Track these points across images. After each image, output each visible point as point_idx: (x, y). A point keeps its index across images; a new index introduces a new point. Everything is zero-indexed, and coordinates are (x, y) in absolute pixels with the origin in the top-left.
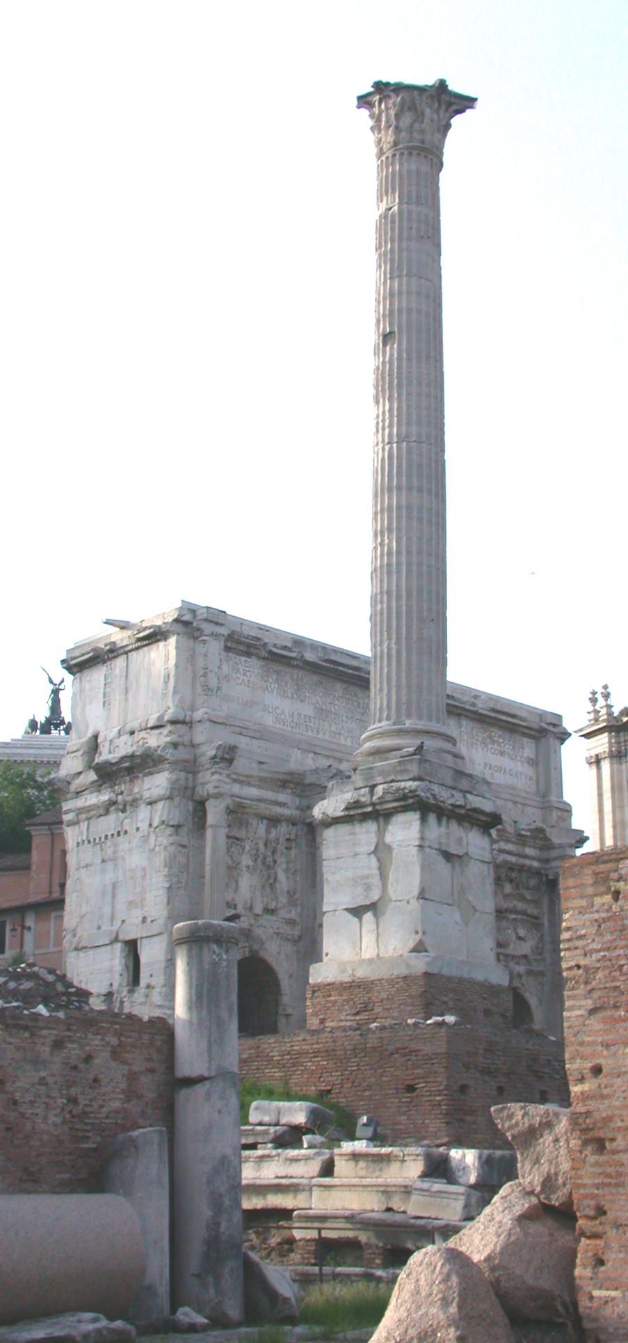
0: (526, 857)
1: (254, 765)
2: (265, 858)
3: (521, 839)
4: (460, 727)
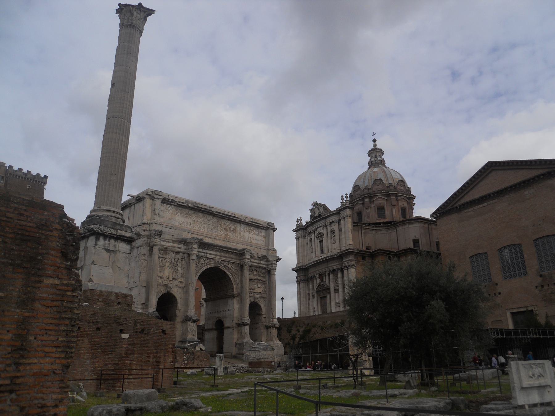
0: (261, 264)
1: (171, 237)
2: (174, 264)
3: (259, 259)
4: (241, 226)
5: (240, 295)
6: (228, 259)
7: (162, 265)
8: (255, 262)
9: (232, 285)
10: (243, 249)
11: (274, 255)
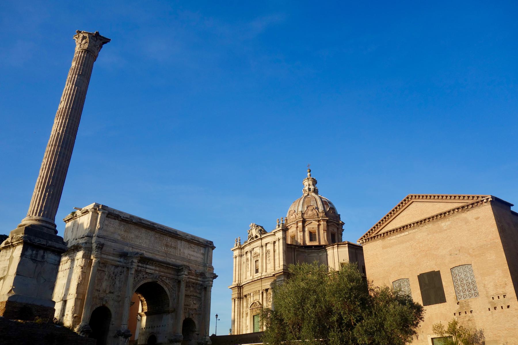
0: (198, 280)
1: (112, 250)
3: (197, 275)
4: (181, 243)
5: (175, 311)
6: (166, 274)
7: (100, 278)
8: (193, 279)
9: (168, 300)
10: (182, 265)
11: (211, 272)
